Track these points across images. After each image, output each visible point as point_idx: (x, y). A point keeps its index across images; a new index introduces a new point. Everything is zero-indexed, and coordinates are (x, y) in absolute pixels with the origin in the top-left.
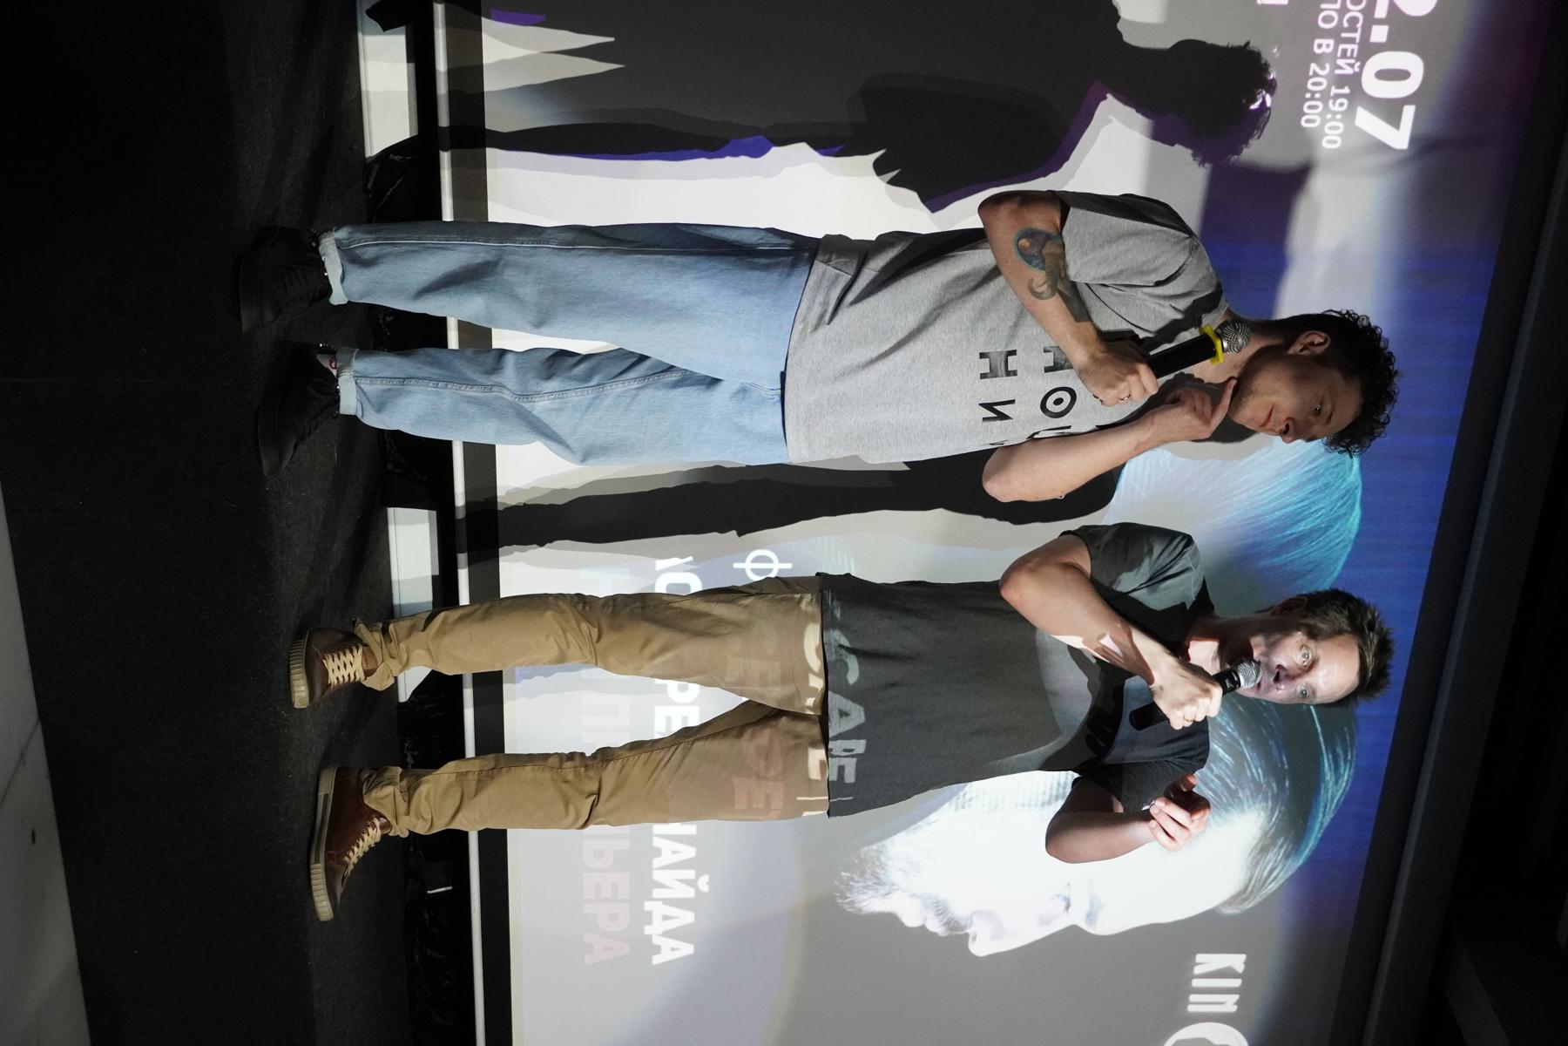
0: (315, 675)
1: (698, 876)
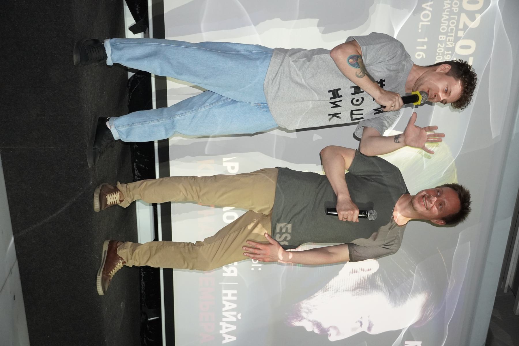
0: (103, 199)
1: (238, 314)
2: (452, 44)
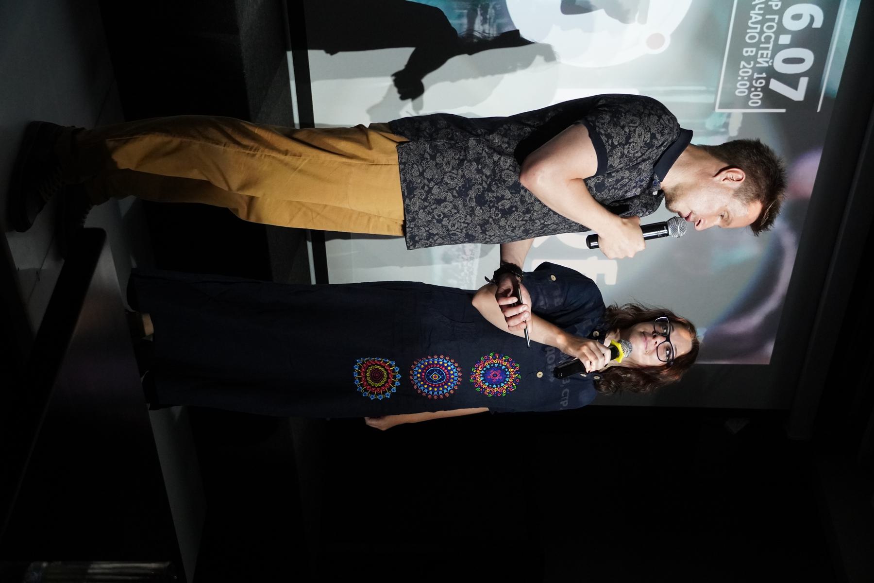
2: (767, 62)
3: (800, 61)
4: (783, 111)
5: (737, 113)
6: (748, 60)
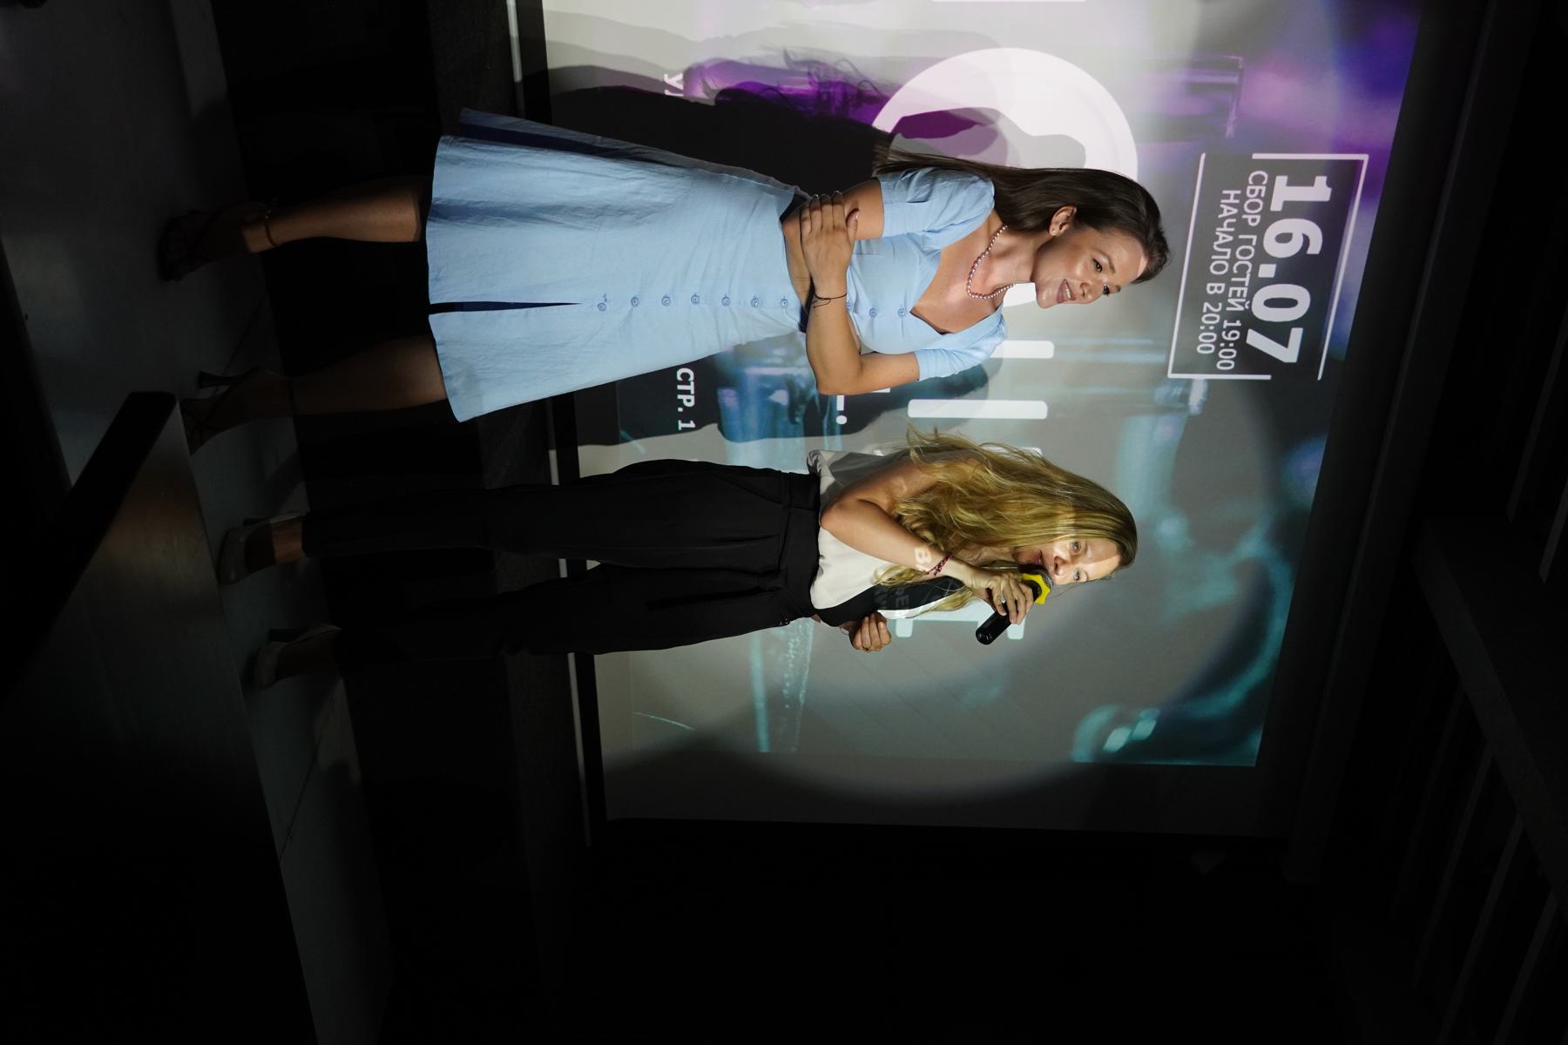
2: (1242, 304)
3: (1291, 303)
4: (1268, 377)
5: (1200, 379)
6: (1214, 300)
